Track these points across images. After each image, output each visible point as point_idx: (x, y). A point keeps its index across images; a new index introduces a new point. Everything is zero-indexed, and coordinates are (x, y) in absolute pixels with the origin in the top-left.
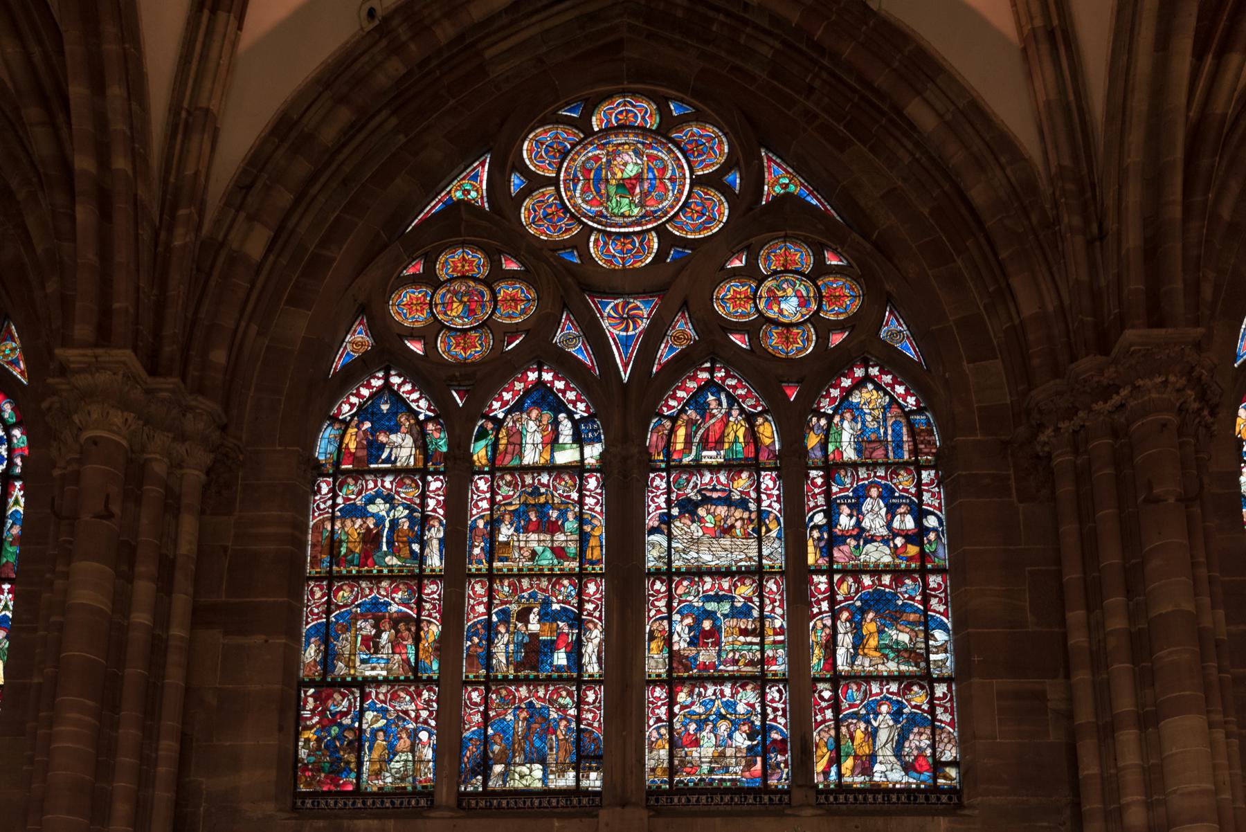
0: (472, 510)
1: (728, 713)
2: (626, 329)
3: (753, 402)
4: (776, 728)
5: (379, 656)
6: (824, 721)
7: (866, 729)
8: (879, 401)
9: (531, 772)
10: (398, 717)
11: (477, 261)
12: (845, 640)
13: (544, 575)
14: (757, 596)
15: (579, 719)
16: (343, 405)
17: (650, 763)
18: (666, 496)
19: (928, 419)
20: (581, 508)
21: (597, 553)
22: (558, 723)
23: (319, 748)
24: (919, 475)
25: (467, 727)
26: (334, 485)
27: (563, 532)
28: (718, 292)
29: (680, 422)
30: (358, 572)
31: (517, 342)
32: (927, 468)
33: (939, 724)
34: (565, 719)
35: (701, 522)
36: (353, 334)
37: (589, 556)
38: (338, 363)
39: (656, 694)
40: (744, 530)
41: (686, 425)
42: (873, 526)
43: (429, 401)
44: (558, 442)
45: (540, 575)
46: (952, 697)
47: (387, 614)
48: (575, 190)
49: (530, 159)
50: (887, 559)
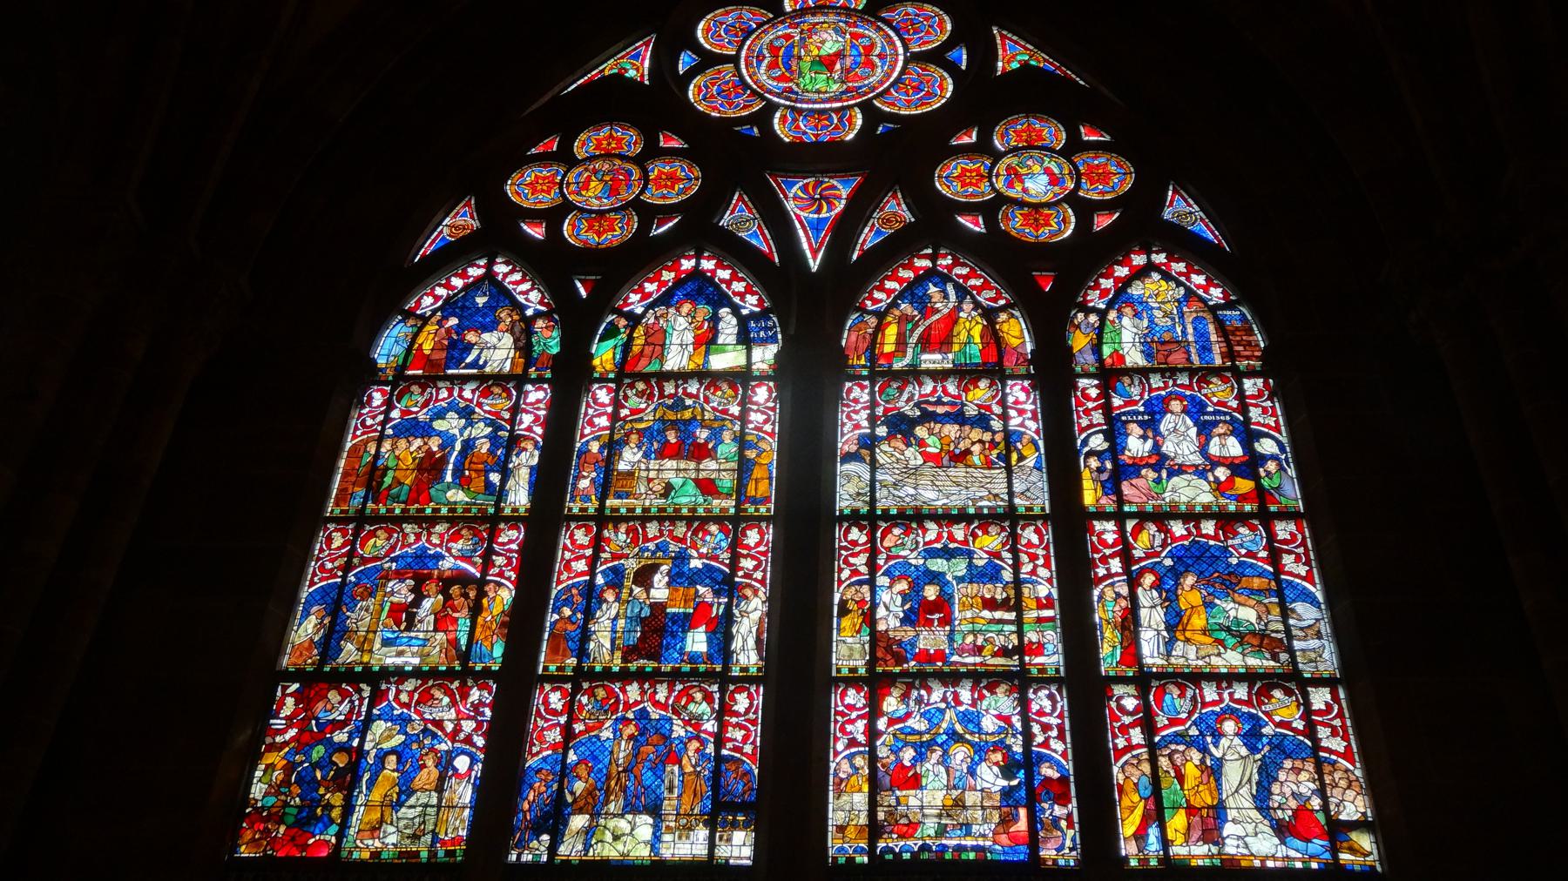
0: (583, 428)
1: (966, 731)
2: (819, 211)
3: (992, 294)
4: (1049, 759)
5: (413, 634)
6: (1130, 748)
7: (1203, 761)
8: (1171, 293)
9: (632, 830)
10: (425, 731)
11: (630, 140)
12: (1152, 617)
13: (682, 518)
14: (1008, 551)
15: (720, 740)
16: (425, 297)
17: (835, 817)
18: (868, 412)
19: (1243, 315)
20: (743, 427)
21: (763, 488)
22: (685, 744)
23: (286, 782)
24: (1240, 385)
25: (535, 750)
26: (391, 394)
27: (715, 458)
28: (941, 170)
29: (889, 319)
30: (403, 511)
31: (671, 224)
32: (1252, 374)
33: (1327, 755)
34: (698, 738)
35: (920, 446)
36: (455, 217)
37: (751, 491)
38: (428, 248)
39: (848, 700)
40: (986, 457)
41: (898, 323)
42: (1180, 452)
43: (542, 293)
44: (715, 343)
45: (673, 519)
46: (1341, 708)
47: (436, 572)
48: (759, 67)
49: (705, 38)
50: (1207, 498)
